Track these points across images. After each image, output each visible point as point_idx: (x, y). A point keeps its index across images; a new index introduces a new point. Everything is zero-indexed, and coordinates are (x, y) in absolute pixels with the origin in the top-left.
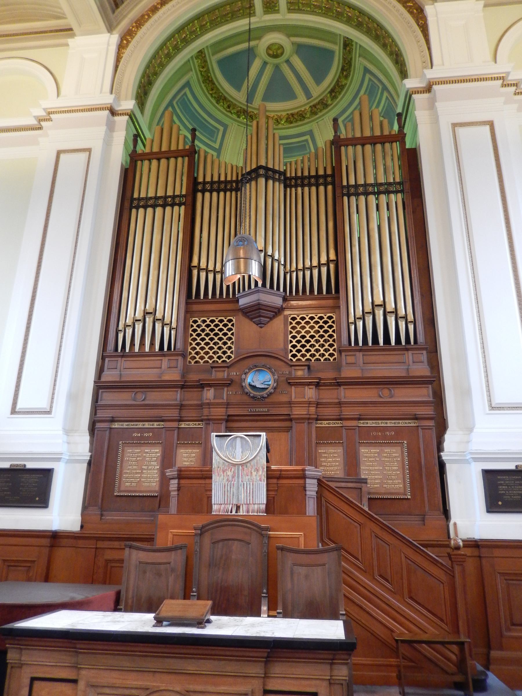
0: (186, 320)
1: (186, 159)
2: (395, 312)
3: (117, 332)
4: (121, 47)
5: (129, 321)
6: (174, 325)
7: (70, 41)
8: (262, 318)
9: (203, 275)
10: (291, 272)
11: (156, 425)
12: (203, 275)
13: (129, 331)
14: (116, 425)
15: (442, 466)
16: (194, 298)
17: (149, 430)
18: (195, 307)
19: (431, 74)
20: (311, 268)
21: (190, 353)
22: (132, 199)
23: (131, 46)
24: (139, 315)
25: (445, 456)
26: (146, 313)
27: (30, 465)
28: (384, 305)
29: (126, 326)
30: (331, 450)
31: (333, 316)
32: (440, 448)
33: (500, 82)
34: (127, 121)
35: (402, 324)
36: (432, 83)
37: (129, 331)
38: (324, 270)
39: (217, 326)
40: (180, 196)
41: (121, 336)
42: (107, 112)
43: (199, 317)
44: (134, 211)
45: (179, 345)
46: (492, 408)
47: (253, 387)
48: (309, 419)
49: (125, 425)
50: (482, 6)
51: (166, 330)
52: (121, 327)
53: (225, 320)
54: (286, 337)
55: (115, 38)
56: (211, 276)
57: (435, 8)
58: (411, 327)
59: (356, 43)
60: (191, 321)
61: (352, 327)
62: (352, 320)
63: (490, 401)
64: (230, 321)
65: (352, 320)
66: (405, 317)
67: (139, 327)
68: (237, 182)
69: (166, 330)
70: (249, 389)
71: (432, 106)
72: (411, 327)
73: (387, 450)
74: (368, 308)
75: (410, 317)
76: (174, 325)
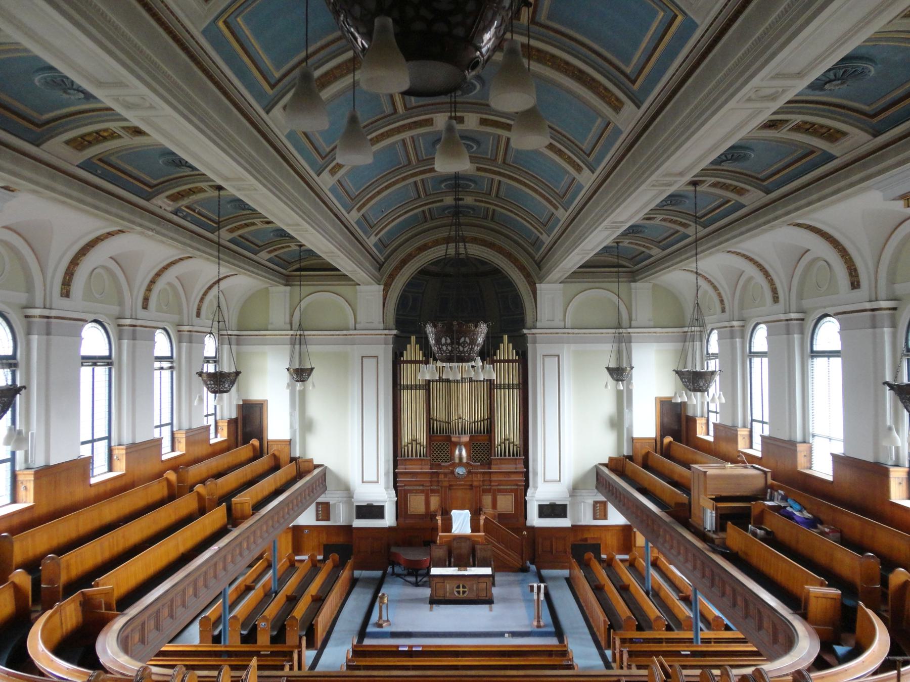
0: (430, 444)
2: (513, 443)
3: (401, 448)
5: (406, 444)
9: (435, 423)
11: (421, 488)
13: (406, 448)
14: (406, 488)
15: (526, 502)
17: (419, 490)
20: (480, 421)
24: (410, 441)
25: (527, 498)
27: (375, 504)
28: (509, 440)
30: (488, 497)
32: (525, 495)
37: (406, 448)
38: (486, 422)
41: (403, 450)
46: (545, 481)
47: (459, 474)
48: (479, 487)
49: (409, 488)
55: (382, 287)
58: (518, 449)
63: (544, 479)
66: (517, 445)
67: (410, 446)
69: (422, 448)
70: (457, 475)
71: (535, 342)
72: (518, 449)
73: (507, 496)
75: (518, 445)
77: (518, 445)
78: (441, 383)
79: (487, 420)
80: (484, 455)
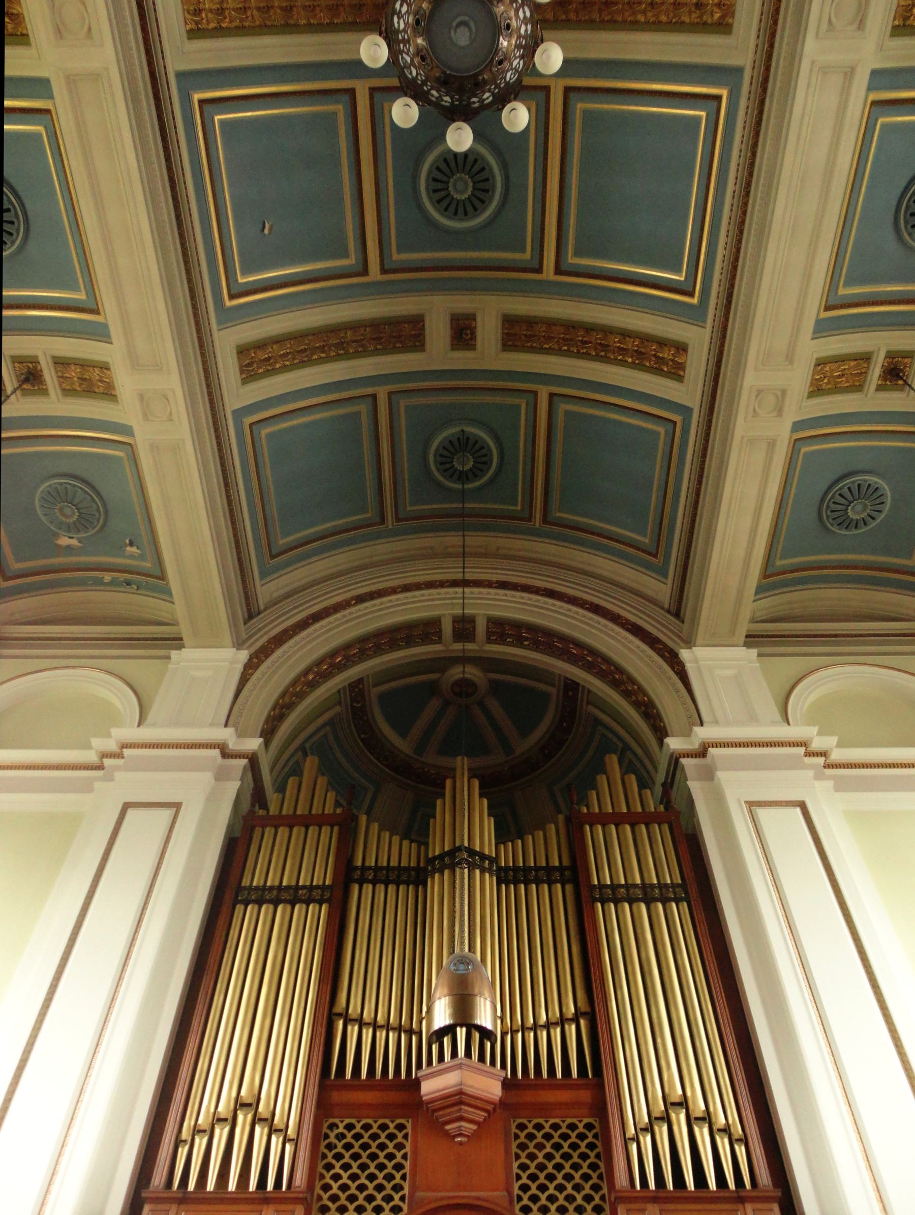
1: (336, 829)
4: (250, 667)
6: (291, 1132)
7: (174, 654)
8: (463, 1124)
9: (353, 1030)
10: (514, 1032)
12: (353, 1030)
13: (201, 1143)
16: (333, 1077)
18: (336, 1096)
19: (703, 733)
20: (548, 1026)
21: (320, 1198)
22: (239, 889)
23: (262, 668)
26: (240, 1104)
28: (684, 1103)
29: (197, 1131)
31: (594, 1123)
33: (802, 750)
34: (245, 767)
35: (723, 1144)
36: (707, 745)
37: (201, 1143)
39: (374, 1137)
40: (323, 887)
41: (183, 1152)
42: (216, 752)
43: (342, 1117)
44: (240, 908)
45: (300, 1179)
50: (756, 654)
51: (276, 1141)
52: (185, 1134)
53: (392, 1126)
54: (508, 1168)
55: (243, 656)
56: (368, 1034)
57: (693, 653)
58: (741, 1151)
59: (584, 687)
60: (326, 1125)
61: (634, 1147)
62: (631, 1131)
64: (400, 1127)
65: (631, 1131)
66: (726, 1130)
68: (418, 869)
69: (276, 1141)
71: (709, 775)
72: (741, 1151)
74: (659, 1107)
75: (737, 1130)
76: (291, 1132)
77: (737, 1130)
78: (392, 888)
79: (576, 1019)
80: (578, 1188)
